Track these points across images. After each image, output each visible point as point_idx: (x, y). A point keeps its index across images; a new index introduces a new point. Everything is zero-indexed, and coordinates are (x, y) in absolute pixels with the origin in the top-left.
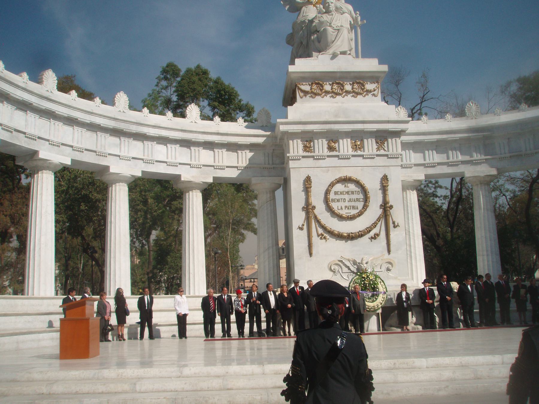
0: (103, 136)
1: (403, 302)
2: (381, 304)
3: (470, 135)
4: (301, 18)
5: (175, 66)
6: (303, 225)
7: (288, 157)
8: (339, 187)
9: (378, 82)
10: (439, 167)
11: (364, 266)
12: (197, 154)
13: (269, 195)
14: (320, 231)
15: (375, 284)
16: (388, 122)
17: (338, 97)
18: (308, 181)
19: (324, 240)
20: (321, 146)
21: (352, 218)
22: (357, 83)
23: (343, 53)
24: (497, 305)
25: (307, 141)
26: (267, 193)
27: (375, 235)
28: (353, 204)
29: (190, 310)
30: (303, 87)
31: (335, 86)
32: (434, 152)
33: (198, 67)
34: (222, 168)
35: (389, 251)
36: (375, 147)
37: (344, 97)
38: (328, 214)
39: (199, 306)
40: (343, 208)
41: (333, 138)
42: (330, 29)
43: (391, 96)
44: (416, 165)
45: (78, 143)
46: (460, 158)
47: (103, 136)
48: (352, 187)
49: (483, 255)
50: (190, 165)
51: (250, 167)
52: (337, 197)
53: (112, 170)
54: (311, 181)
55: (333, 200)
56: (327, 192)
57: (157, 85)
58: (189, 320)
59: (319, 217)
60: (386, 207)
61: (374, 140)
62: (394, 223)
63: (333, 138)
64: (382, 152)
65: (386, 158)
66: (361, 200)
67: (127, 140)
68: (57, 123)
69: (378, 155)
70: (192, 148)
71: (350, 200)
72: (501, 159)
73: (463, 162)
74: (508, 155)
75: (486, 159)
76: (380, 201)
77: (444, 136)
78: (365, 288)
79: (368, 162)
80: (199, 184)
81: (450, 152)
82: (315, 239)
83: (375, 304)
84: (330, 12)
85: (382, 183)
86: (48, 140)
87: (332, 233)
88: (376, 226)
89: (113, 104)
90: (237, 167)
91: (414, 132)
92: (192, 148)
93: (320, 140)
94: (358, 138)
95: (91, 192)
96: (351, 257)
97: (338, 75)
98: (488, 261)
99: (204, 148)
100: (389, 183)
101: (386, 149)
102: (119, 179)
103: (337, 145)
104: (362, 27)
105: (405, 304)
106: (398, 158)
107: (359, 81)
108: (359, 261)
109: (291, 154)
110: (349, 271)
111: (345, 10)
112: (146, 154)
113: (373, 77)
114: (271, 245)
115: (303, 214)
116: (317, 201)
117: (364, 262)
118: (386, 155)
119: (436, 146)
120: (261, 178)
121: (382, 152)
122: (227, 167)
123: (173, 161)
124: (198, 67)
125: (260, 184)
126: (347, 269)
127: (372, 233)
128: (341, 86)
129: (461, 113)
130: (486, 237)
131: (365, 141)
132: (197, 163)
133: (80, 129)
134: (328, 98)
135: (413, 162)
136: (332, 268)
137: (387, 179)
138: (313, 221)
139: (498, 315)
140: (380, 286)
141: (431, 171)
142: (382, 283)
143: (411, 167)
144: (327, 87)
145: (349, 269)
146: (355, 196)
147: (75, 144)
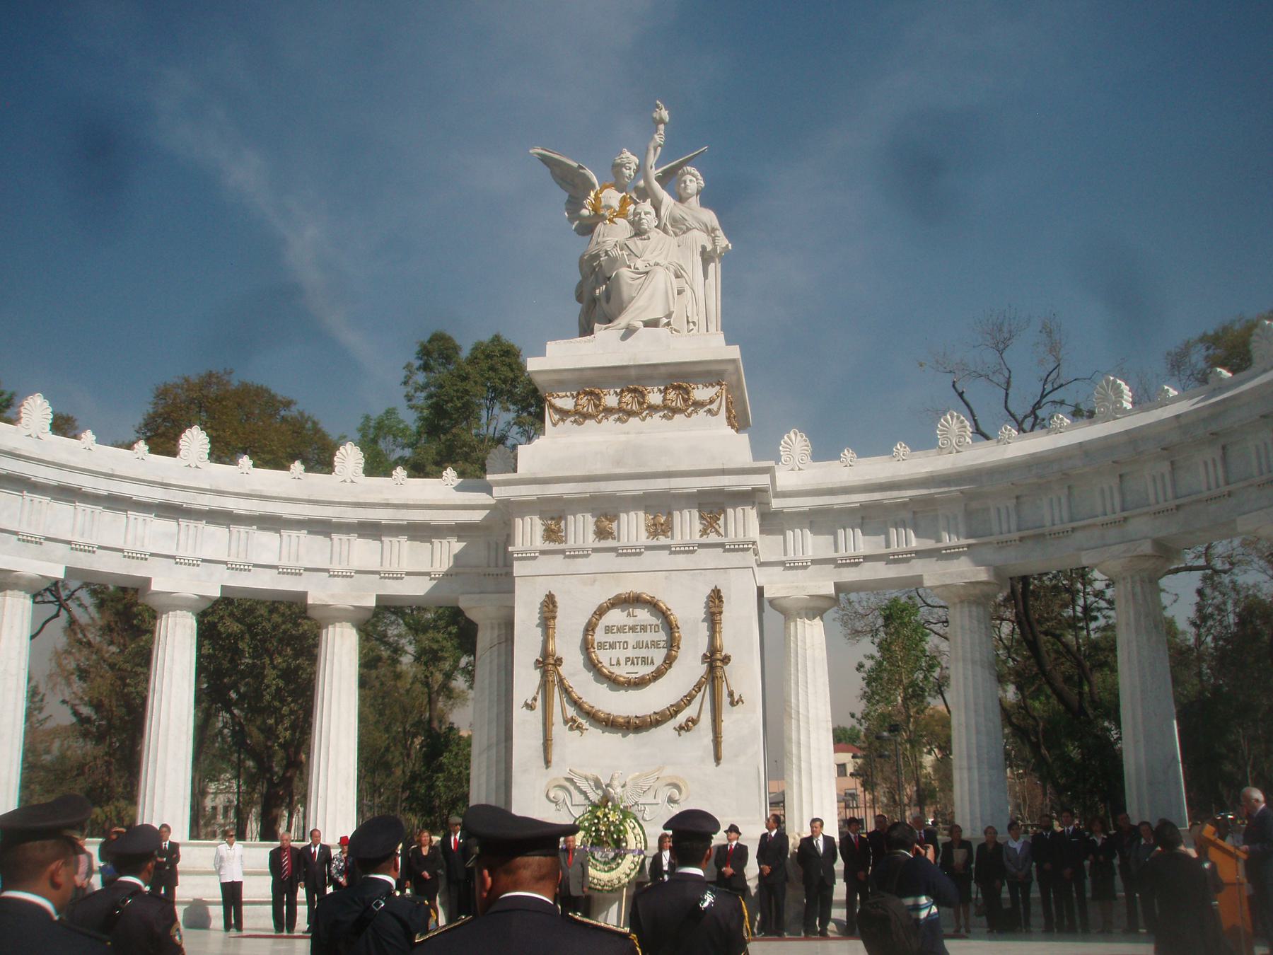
0: (140, 519)
1: (661, 873)
2: (628, 875)
3: (933, 491)
4: (593, 249)
5: (449, 339)
6: (535, 699)
7: (512, 553)
8: (616, 617)
9: (719, 384)
10: (868, 565)
11: (616, 791)
12: (345, 547)
13: (496, 632)
14: (571, 712)
15: (620, 831)
16: (724, 472)
17: (631, 419)
18: (549, 605)
19: (577, 732)
20: (581, 528)
21: (640, 683)
22: (675, 388)
23: (653, 323)
24: (974, 886)
25: (552, 519)
26: (492, 628)
27: (688, 720)
28: (643, 653)
29: (245, 874)
30: (558, 403)
31: (628, 397)
32: (858, 532)
33: (497, 339)
34: (396, 577)
35: (718, 758)
36: (698, 526)
37: (644, 419)
38: (589, 676)
39: (266, 867)
40: (623, 661)
41: (606, 511)
42: (625, 273)
43: (987, 377)
44: (814, 562)
45: (82, 535)
46: (914, 543)
47: (140, 519)
48: (643, 615)
49: (961, 769)
50: (327, 570)
51: (457, 574)
52: (611, 638)
53: (155, 587)
54: (555, 607)
55: (601, 646)
56: (590, 628)
57: (405, 383)
58: (247, 894)
59: (569, 682)
60: (715, 660)
61: (695, 513)
62: (731, 694)
63: (606, 511)
64: (713, 538)
65: (721, 550)
66: (662, 644)
67: (192, 524)
68: (37, 498)
69: (701, 546)
70: (334, 536)
71: (638, 646)
72: (1002, 545)
73: (920, 554)
74: (1016, 535)
75: (969, 546)
76: (703, 648)
77: (877, 496)
78: (598, 843)
79: (681, 561)
80: (345, 610)
81: (893, 531)
82: (558, 729)
83: (613, 875)
84: (645, 232)
85: (708, 607)
86: (16, 533)
87: (593, 716)
88: (690, 702)
89: (172, 452)
90: (428, 574)
91: (824, 486)
92: (334, 536)
93: (579, 516)
94: (660, 508)
95: (222, 618)
96: (592, 772)
97: (633, 372)
98: (970, 783)
99: (360, 536)
100: (725, 608)
101: (722, 531)
102: (175, 603)
103: (614, 525)
104: (728, 260)
105: (666, 877)
106: (748, 549)
107: (677, 385)
108: (604, 781)
109: (517, 547)
110: (587, 802)
111: (691, 222)
112: (234, 551)
113: (710, 373)
114: (494, 740)
115: (536, 676)
116: (567, 647)
117: (615, 783)
118: (722, 545)
119: (863, 518)
120: (477, 596)
121: (713, 538)
122: (408, 574)
123: (293, 563)
124: (497, 339)
125: (478, 609)
126: (582, 797)
127: (681, 718)
128: (639, 394)
129: (924, 441)
130: (967, 727)
131: (676, 514)
132: (344, 566)
133: (89, 508)
134: (610, 423)
135: (810, 554)
136: (552, 795)
137: (720, 599)
138: (556, 689)
139: (1037, 909)
140: (630, 836)
141: (849, 575)
142: (638, 830)
143: (806, 567)
144: (611, 400)
145: (587, 798)
146: (647, 637)
147: (76, 538)
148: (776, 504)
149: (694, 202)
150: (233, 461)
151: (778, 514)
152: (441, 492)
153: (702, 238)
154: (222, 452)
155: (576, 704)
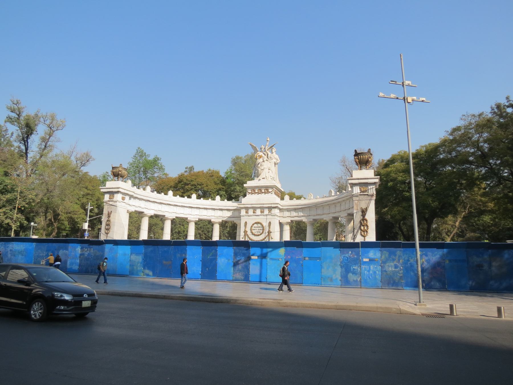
8: (255, 225)
20: (251, 212)
21: (259, 235)
42: (260, 170)
46: (302, 214)
60: (269, 232)
72: (314, 215)
89: (191, 198)
94: (262, 209)
107: (266, 189)
113: (272, 187)
115: (244, 234)
116: (248, 229)
141: (293, 219)
148: (281, 207)
149: (274, 153)
150: (200, 199)
151: (282, 209)
152: (232, 204)
153: (274, 160)
154: (199, 197)
155: (249, 238)
